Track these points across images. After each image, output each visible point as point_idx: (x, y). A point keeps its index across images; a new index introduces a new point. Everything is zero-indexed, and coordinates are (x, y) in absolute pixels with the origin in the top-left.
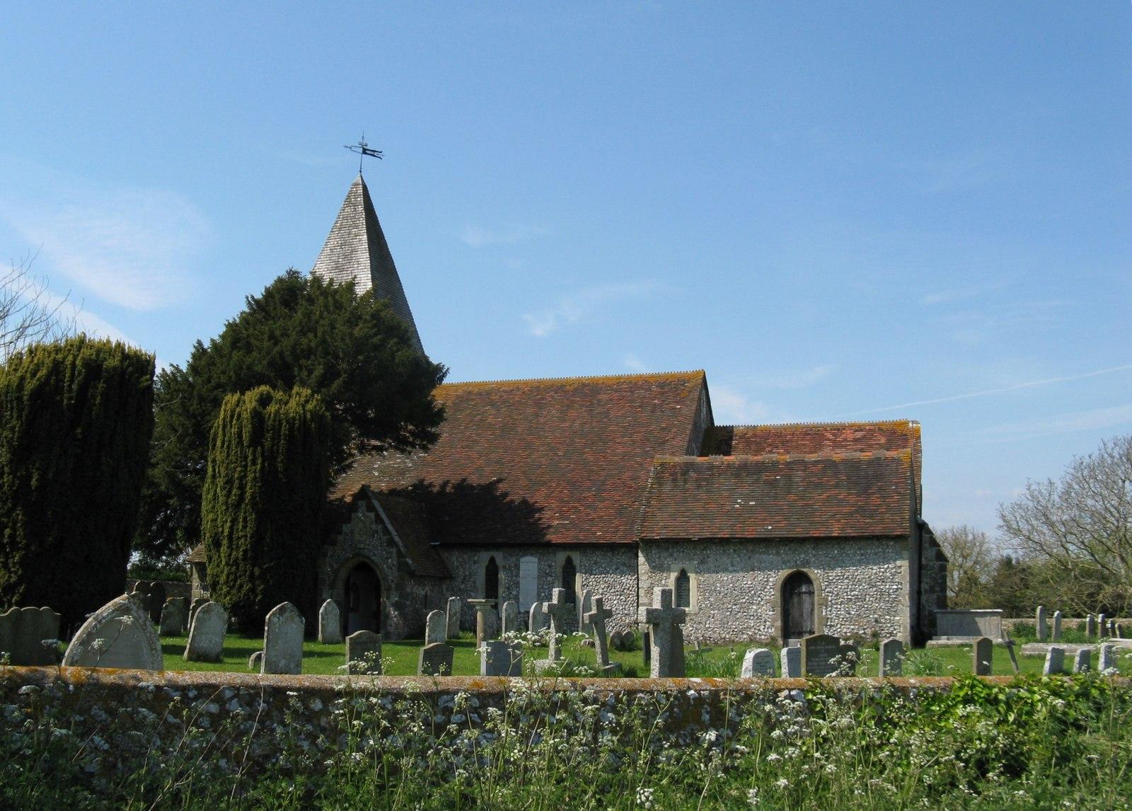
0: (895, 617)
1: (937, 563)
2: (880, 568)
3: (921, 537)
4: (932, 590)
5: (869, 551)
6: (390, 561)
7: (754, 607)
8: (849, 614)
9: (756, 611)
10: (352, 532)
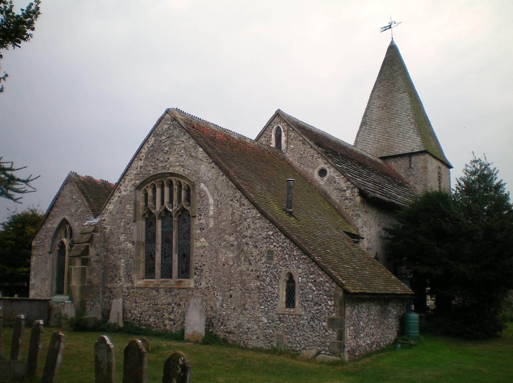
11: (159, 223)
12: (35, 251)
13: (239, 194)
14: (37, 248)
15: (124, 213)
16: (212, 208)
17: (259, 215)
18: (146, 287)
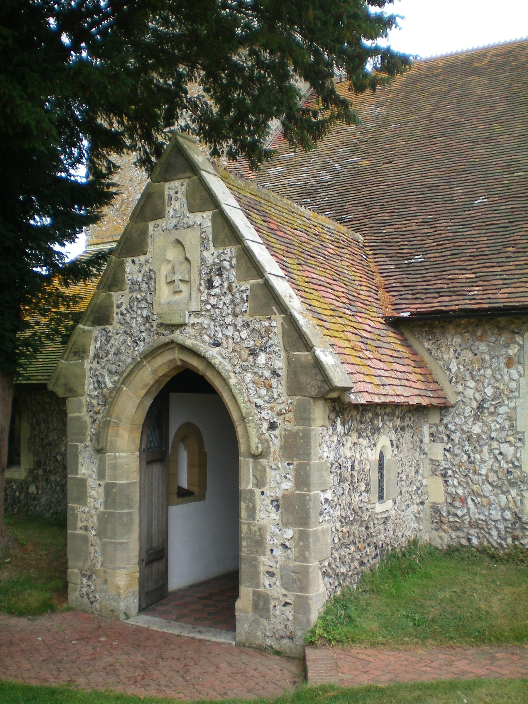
6: (262, 359)
10: (150, 277)
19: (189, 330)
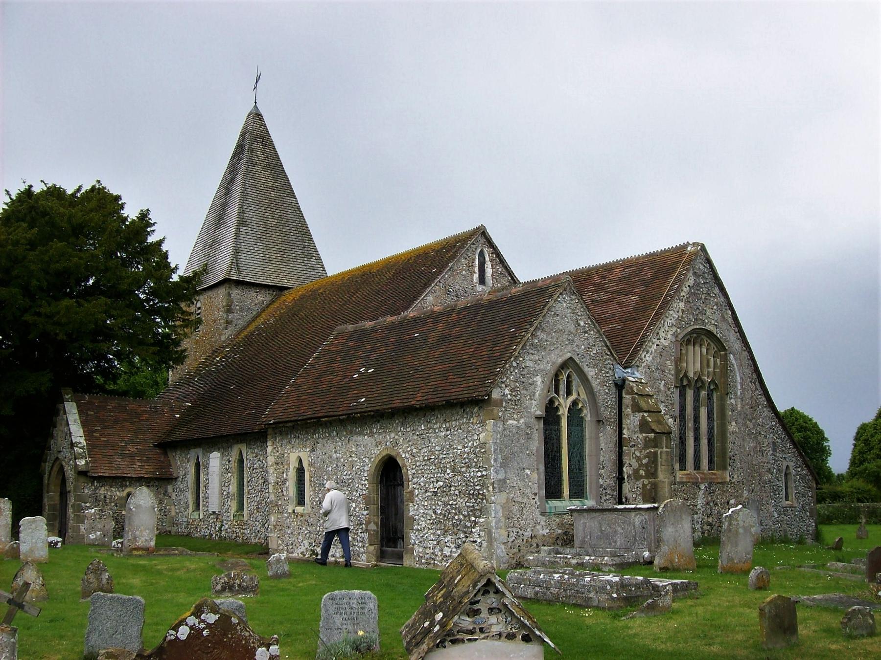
0: (480, 517)
1: (641, 436)
2: (464, 447)
3: (620, 398)
4: (636, 476)
5: (454, 423)
7: (354, 505)
8: (435, 513)
9: (355, 508)
11: (690, 394)
12: (501, 411)
13: (755, 377)
14: (504, 404)
15: (664, 371)
16: (739, 388)
17: (766, 403)
18: (689, 482)
19: (62, 453)
